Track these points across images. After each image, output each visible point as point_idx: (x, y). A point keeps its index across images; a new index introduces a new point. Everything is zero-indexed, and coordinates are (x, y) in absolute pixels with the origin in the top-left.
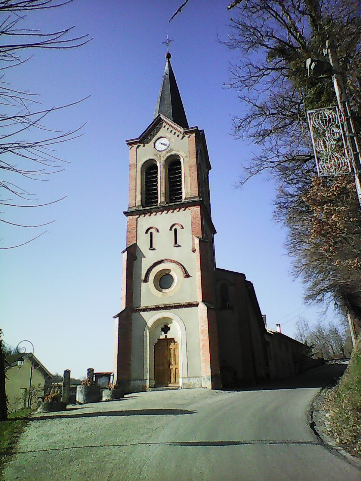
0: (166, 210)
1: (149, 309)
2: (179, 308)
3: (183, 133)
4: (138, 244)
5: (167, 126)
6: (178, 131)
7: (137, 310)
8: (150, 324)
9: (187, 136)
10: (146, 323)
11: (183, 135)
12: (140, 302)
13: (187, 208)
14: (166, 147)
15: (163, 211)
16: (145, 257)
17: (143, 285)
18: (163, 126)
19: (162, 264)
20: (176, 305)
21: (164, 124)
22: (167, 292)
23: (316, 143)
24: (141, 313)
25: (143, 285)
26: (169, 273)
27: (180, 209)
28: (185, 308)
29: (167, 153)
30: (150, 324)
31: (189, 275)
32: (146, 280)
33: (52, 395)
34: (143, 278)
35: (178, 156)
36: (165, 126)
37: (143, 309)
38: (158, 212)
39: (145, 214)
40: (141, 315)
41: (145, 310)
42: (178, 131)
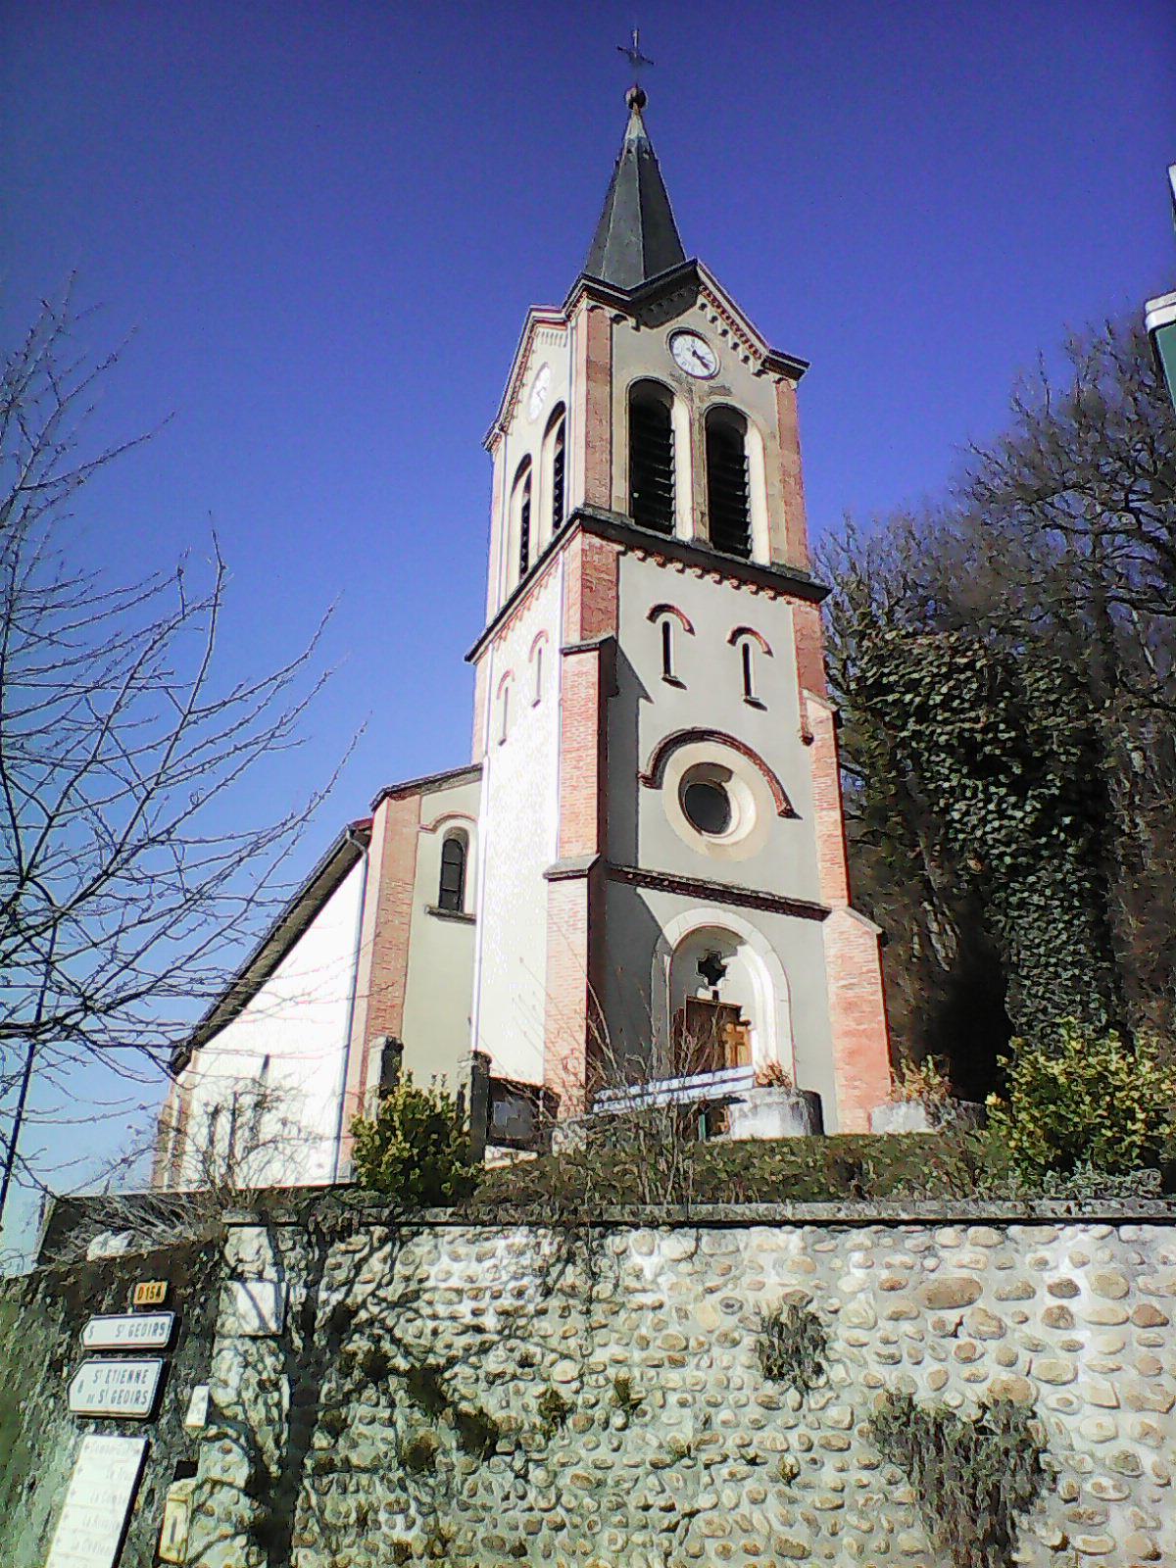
0: (716, 571)
1: (671, 882)
2: (766, 909)
3: (765, 361)
4: (624, 643)
5: (711, 312)
6: (747, 345)
7: (629, 873)
8: (673, 933)
9: (774, 376)
10: (661, 930)
11: (763, 364)
12: (637, 853)
13: (781, 594)
14: (706, 373)
15: (706, 571)
16: (647, 698)
17: (645, 793)
18: (699, 303)
19: (706, 743)
20: (761, 895)
21: (701, 300)
22: (723, 845)
23: (184, 1197)
24: (640, 890)
25: (645, 793)
26: (723, 784)
27: (760, 588)
28: (784, 916)
29: (711, 394)
30: (673, 933)
31: (791, 810)
32: (654, 781)
33: (308, 1495)
34: (645, 767)
35: (745, 419)
36: (703, 306)
37: (652, 877)
38: (690, 567)
39: (648, 553)
40: (639, 896)
41: (658, 882)
42: (747, 345)
